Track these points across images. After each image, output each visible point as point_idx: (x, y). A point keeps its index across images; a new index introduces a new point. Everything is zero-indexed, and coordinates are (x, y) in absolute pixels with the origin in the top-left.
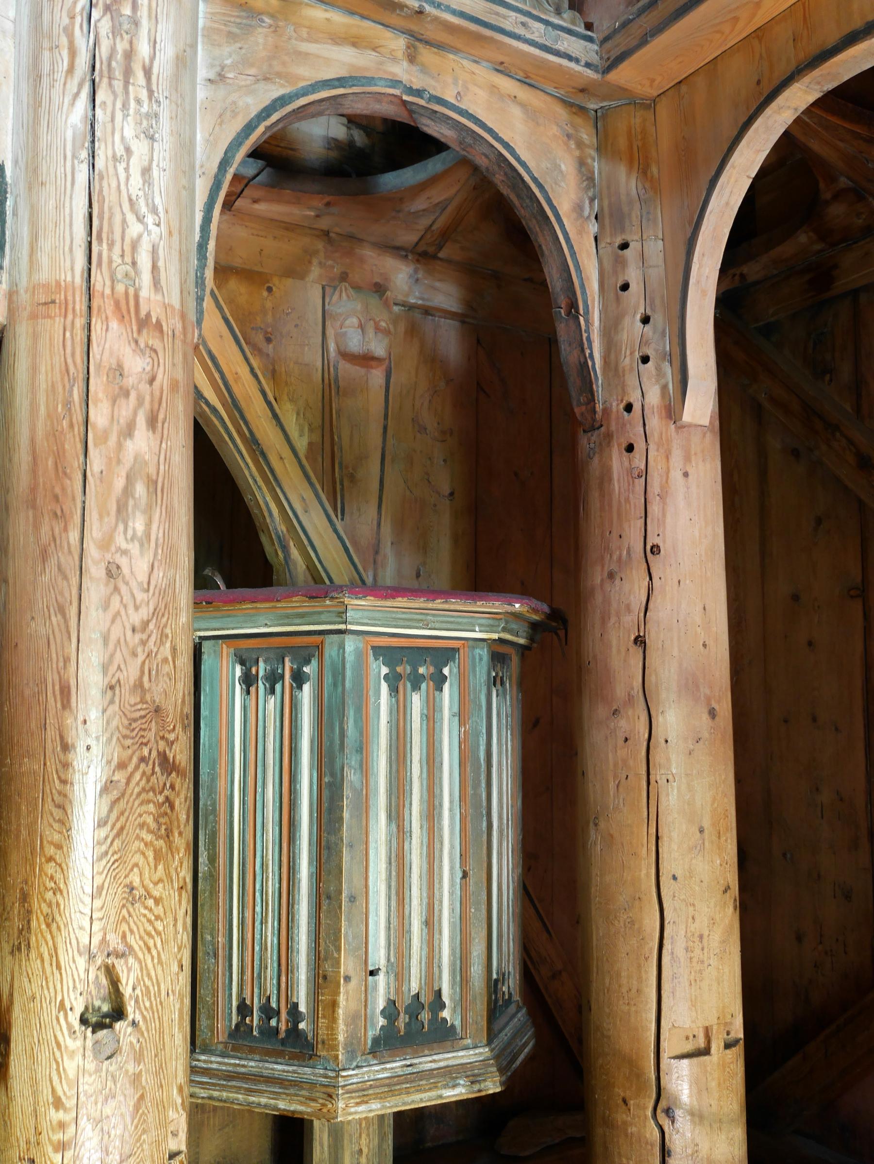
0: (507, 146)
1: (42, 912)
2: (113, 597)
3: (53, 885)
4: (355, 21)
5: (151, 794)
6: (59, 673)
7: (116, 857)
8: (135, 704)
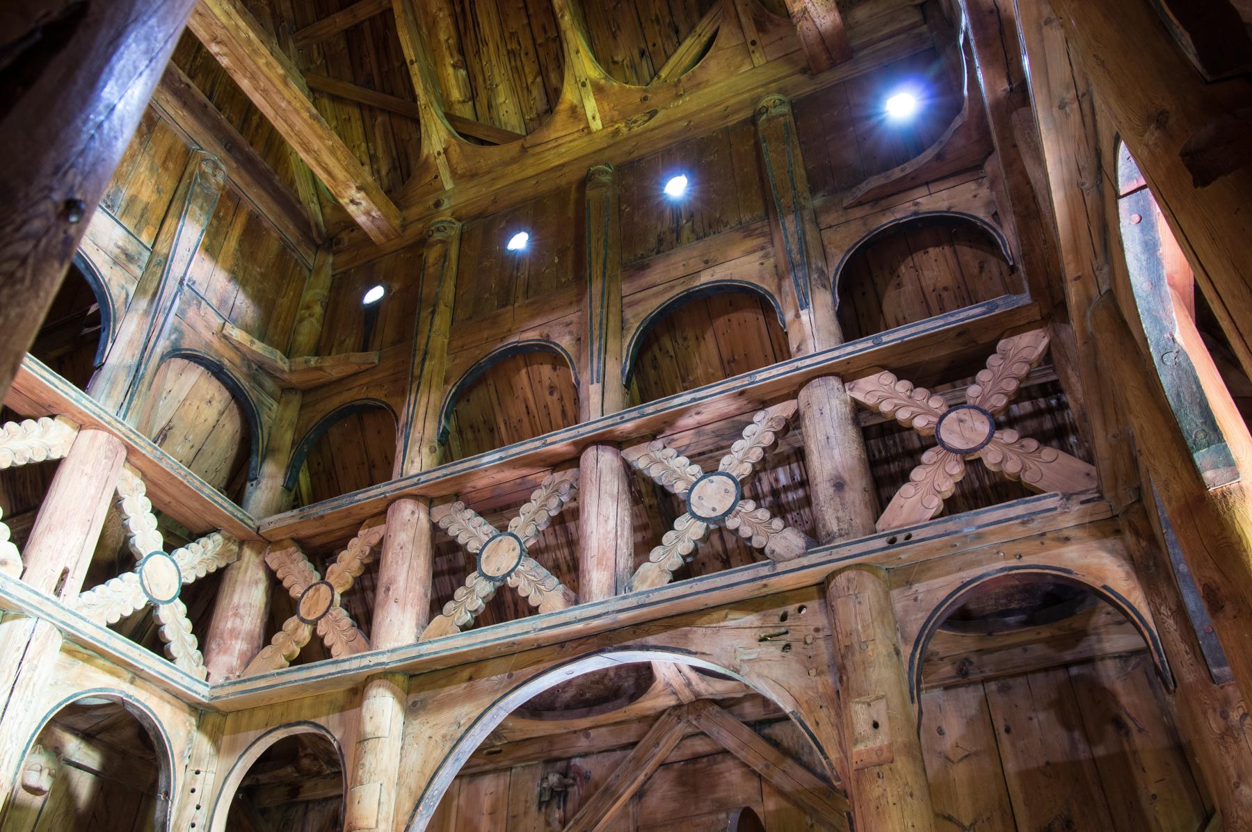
0: (160, 722)
4: (114, 666)
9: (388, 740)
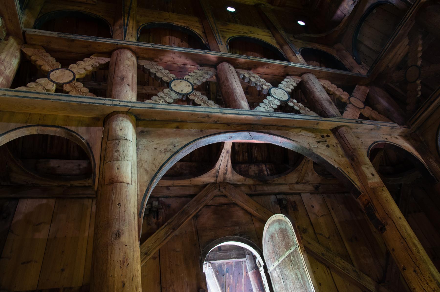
9: (132, 143)
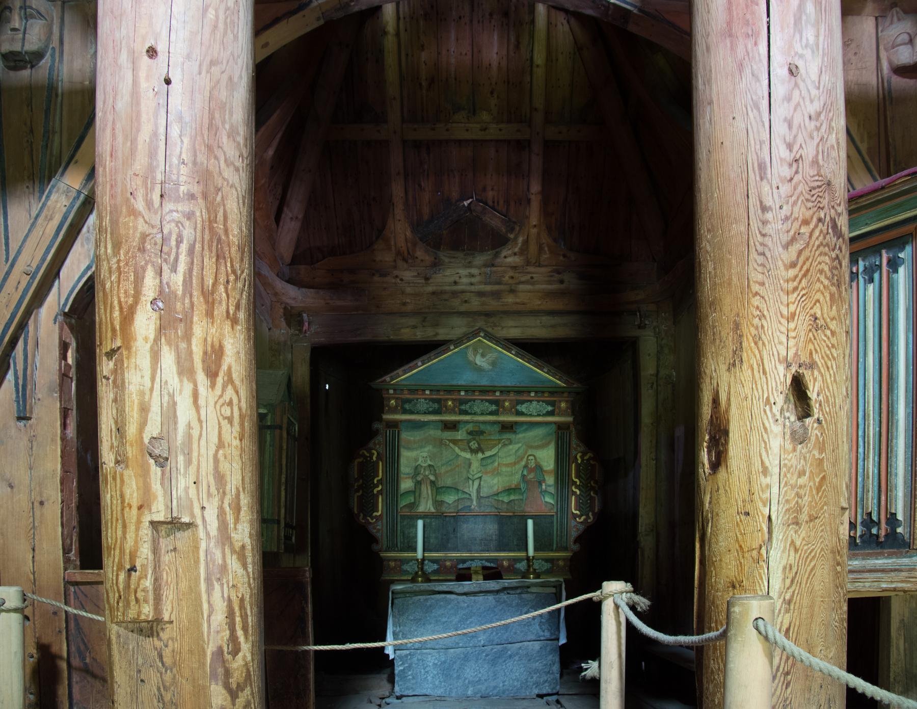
1: (751, 334)
2: (794, 91)
3: (758, 313)
5: (827, 248)
6: (756, 153)
7: (804, 292)
8: (814, 176)
